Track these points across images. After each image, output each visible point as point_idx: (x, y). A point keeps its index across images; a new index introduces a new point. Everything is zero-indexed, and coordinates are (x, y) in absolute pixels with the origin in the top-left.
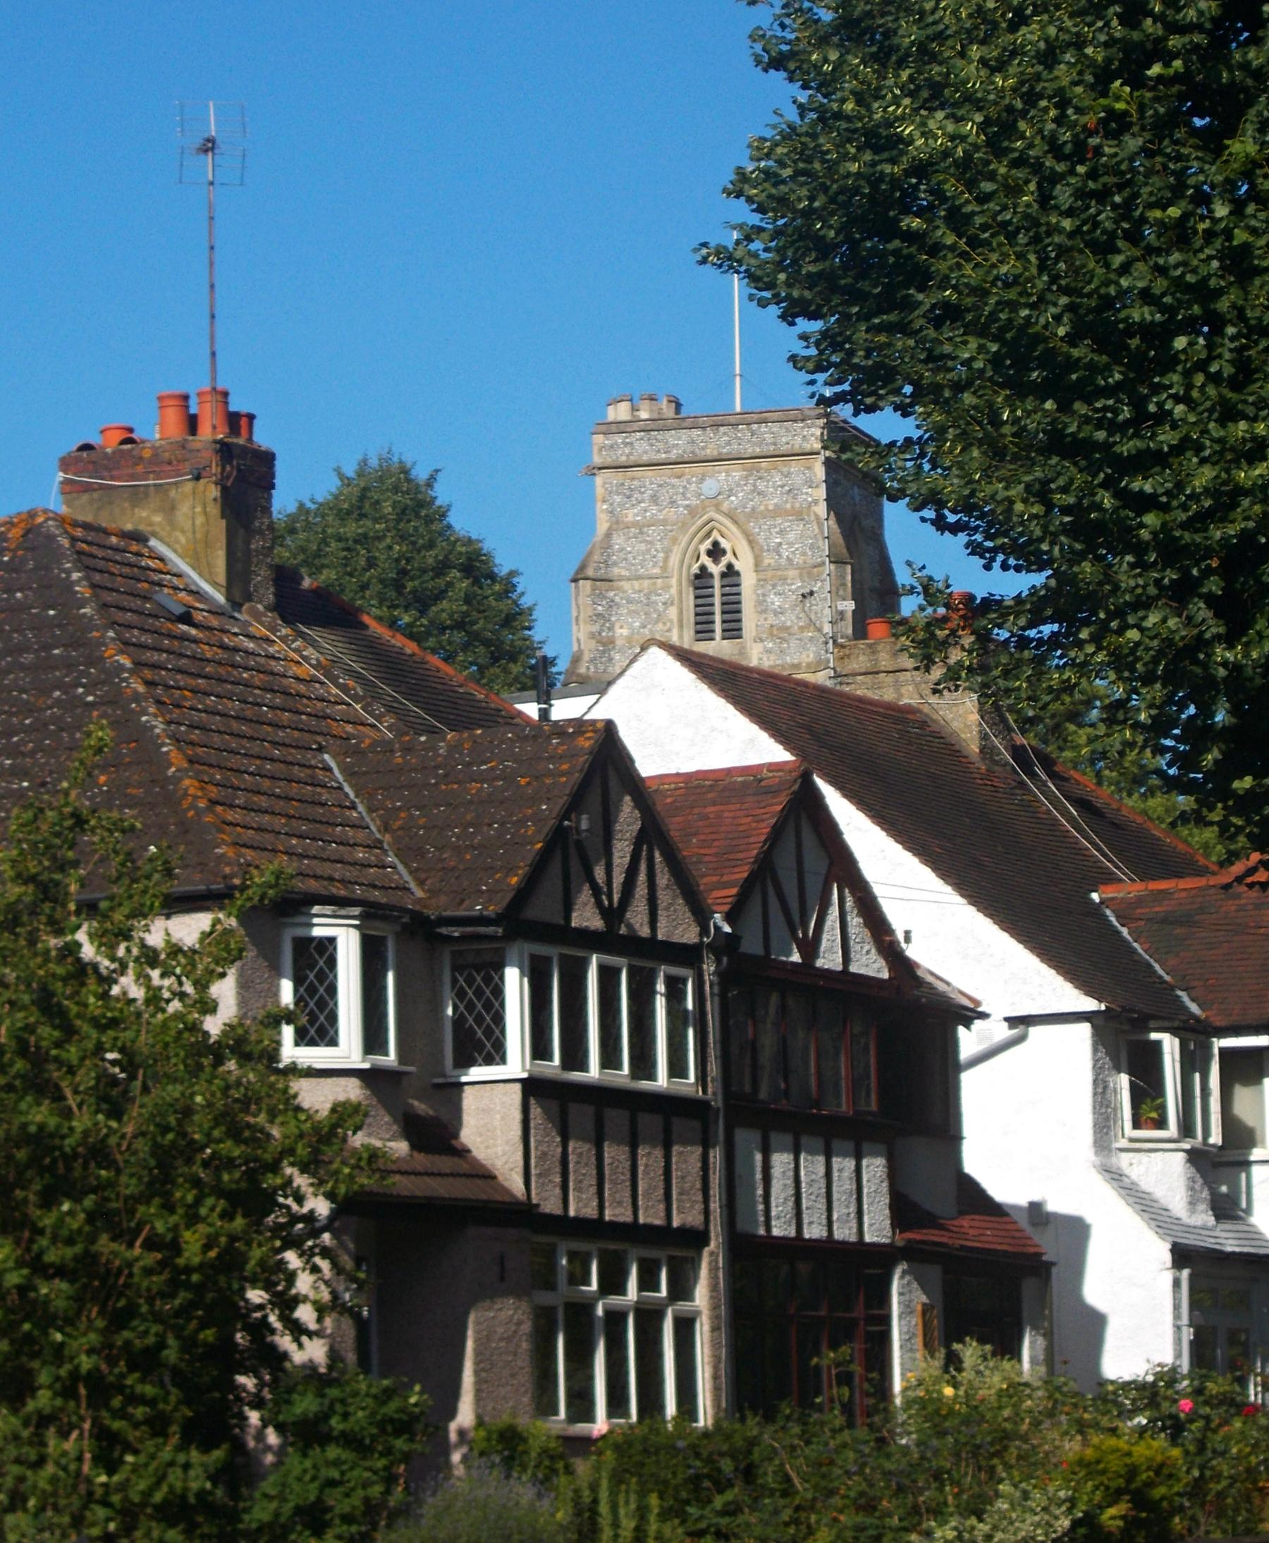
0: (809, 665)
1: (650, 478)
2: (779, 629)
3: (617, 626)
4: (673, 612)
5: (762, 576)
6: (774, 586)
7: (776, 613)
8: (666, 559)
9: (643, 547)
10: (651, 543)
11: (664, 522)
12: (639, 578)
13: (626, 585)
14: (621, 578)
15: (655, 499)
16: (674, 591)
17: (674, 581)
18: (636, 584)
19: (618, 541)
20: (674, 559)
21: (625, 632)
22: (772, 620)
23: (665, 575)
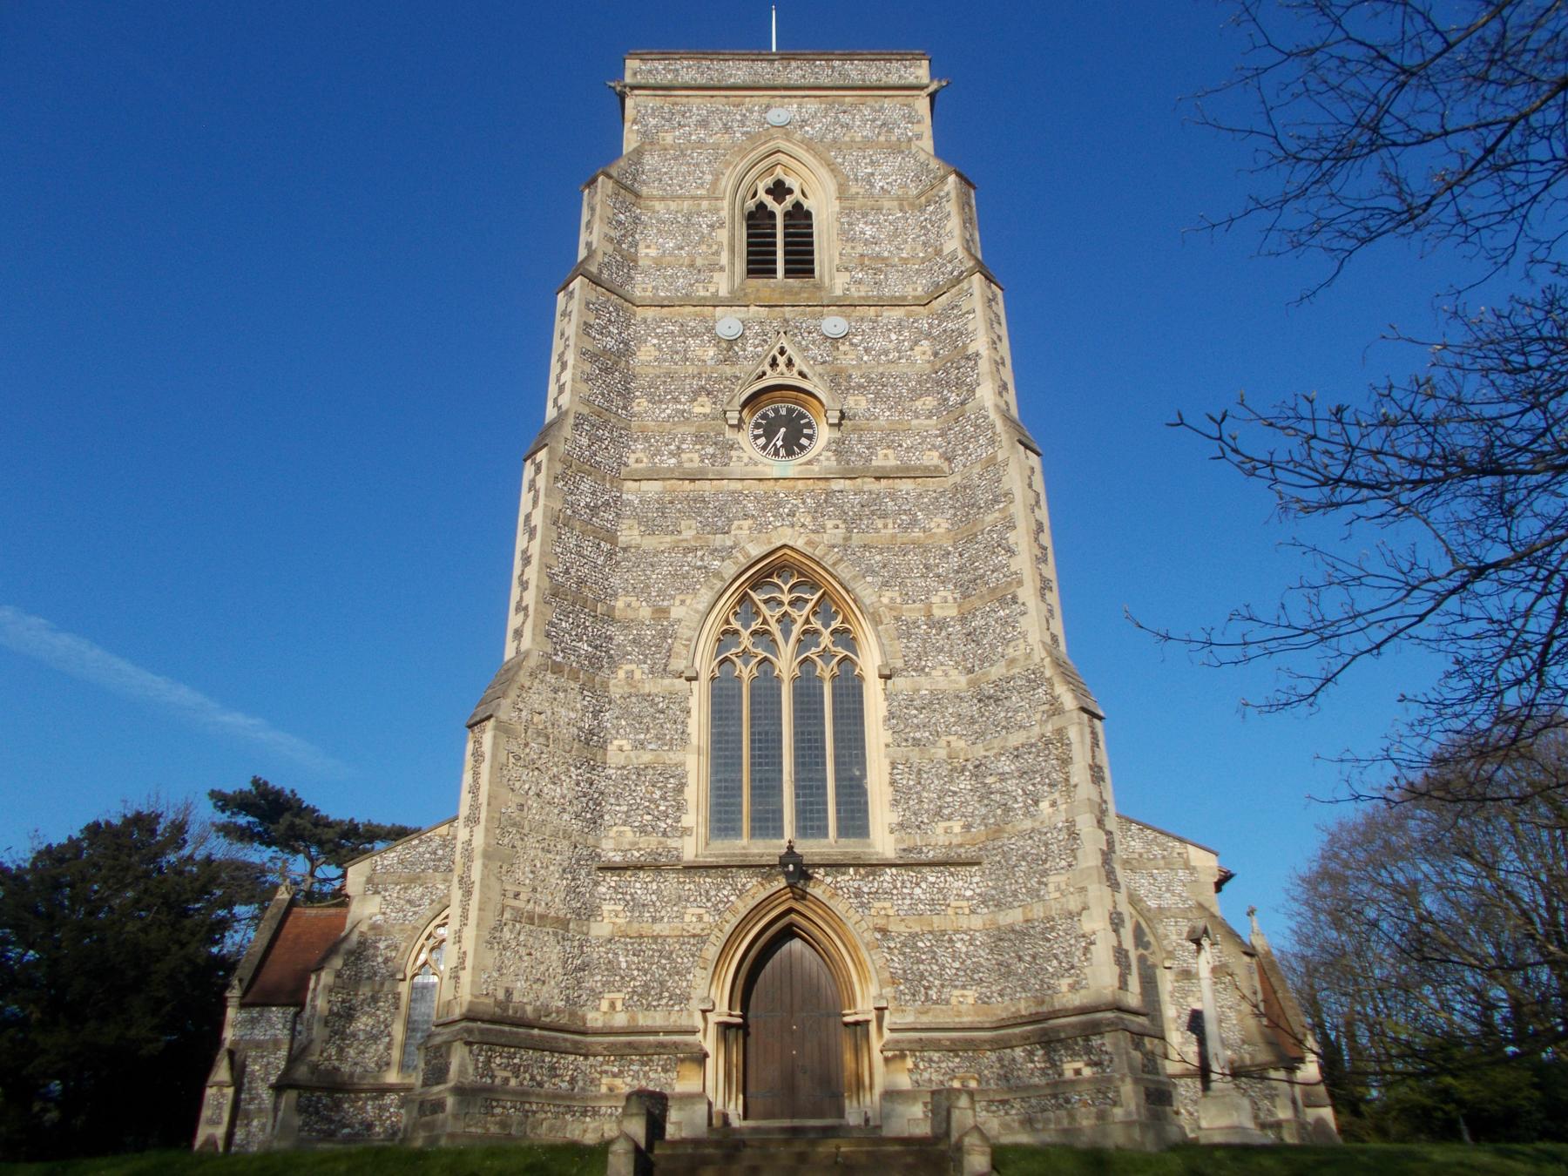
0: (916, 298)
1: (698, 104)
2: (872, 258)
3: (641, 246)
4: (723, 235)
5: (847, 204)
6: (865, 215)
7: (866, 242)
8: (716, 181)
9: (684, 168)
10: (697, 165)
11: (716, 147)
12: (674, 198)
13: (658, 206)
14: (651, 198)
15: (703, 123)
16: (725, 214)
17: (726, 204)
18: (673, 206)
19: (650, 161)
20: (727, 183)
21: (653, 252)
22: (859, 250)
23: (713, 197)
